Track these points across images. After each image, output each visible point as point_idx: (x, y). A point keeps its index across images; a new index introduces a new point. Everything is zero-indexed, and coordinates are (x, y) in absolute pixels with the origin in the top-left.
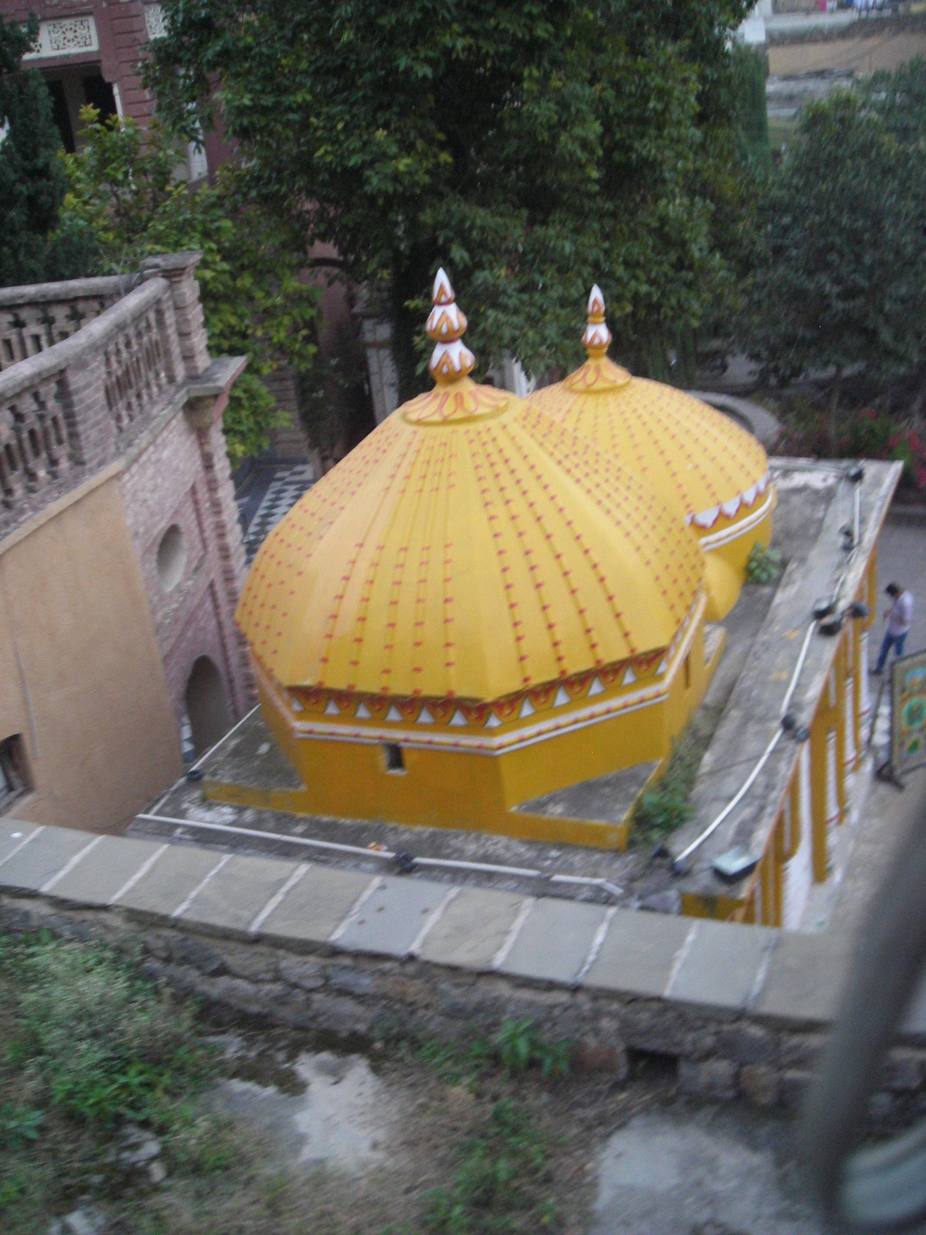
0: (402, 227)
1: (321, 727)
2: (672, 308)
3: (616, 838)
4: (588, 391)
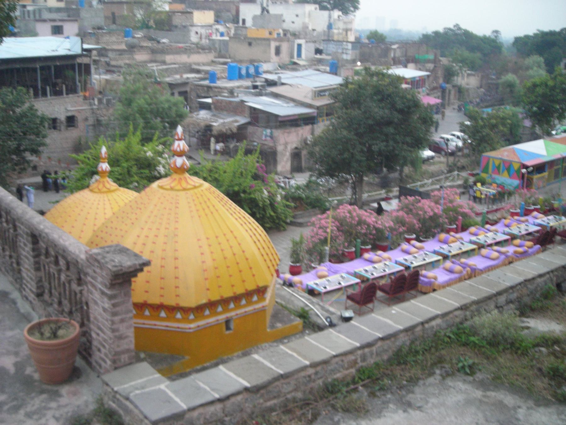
1: (202, 323)
3: (301, 327)
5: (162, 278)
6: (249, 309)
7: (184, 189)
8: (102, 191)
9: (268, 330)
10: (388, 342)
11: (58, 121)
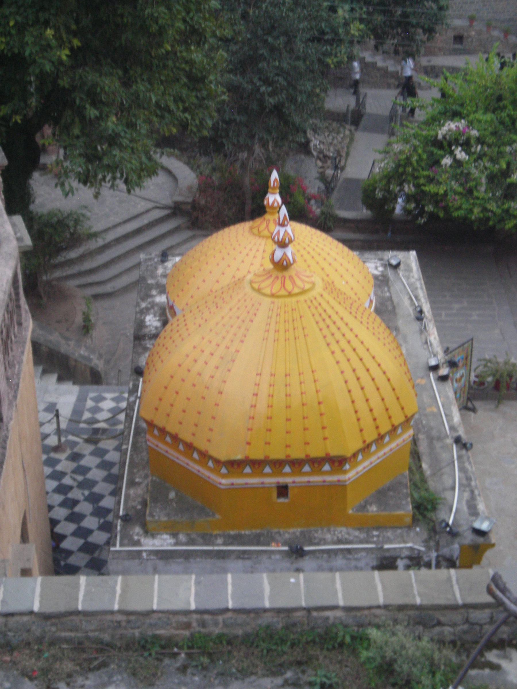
1: (239, 481)
2: (196, 126)
3: (408, 520)
5: (199, 413)
6: (316, 479)
7: (273, 295)
8: (262, 234)
9: (350, 512)
10: (244, 616)
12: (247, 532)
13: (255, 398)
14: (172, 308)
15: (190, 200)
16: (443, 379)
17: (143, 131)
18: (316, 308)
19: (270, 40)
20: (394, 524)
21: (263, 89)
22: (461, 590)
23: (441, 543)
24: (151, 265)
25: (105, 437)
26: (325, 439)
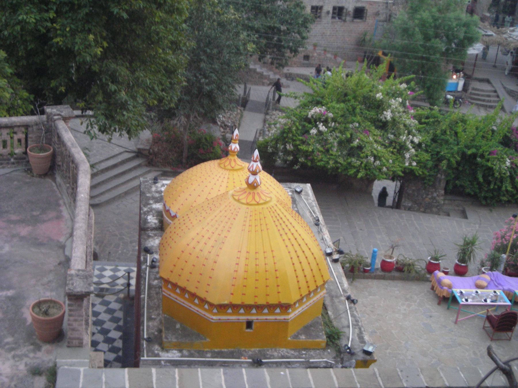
0: (74, 69)
1: (224, 317)
3: (324, 345)
4: (233, 169)
5: (201, 274)
6: (271, 317)
7: (248, 204)
8: (227, 168)
9: (289, 339)
11: (345, 11)
12: (225, 350)
13: (237, 266)
14: (168, 211)
15: (148, 148)
16: (335, 261)
17: (140, 102)
18: (274, 212)
19: (208, 51)
20: (315, 347)
21: (203, 80)
22: (382, 381)
23: (345, 359)
24: (148, 185)
25: (107, 293)
26: (279, 292)
